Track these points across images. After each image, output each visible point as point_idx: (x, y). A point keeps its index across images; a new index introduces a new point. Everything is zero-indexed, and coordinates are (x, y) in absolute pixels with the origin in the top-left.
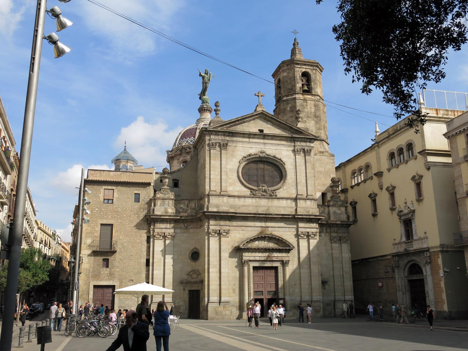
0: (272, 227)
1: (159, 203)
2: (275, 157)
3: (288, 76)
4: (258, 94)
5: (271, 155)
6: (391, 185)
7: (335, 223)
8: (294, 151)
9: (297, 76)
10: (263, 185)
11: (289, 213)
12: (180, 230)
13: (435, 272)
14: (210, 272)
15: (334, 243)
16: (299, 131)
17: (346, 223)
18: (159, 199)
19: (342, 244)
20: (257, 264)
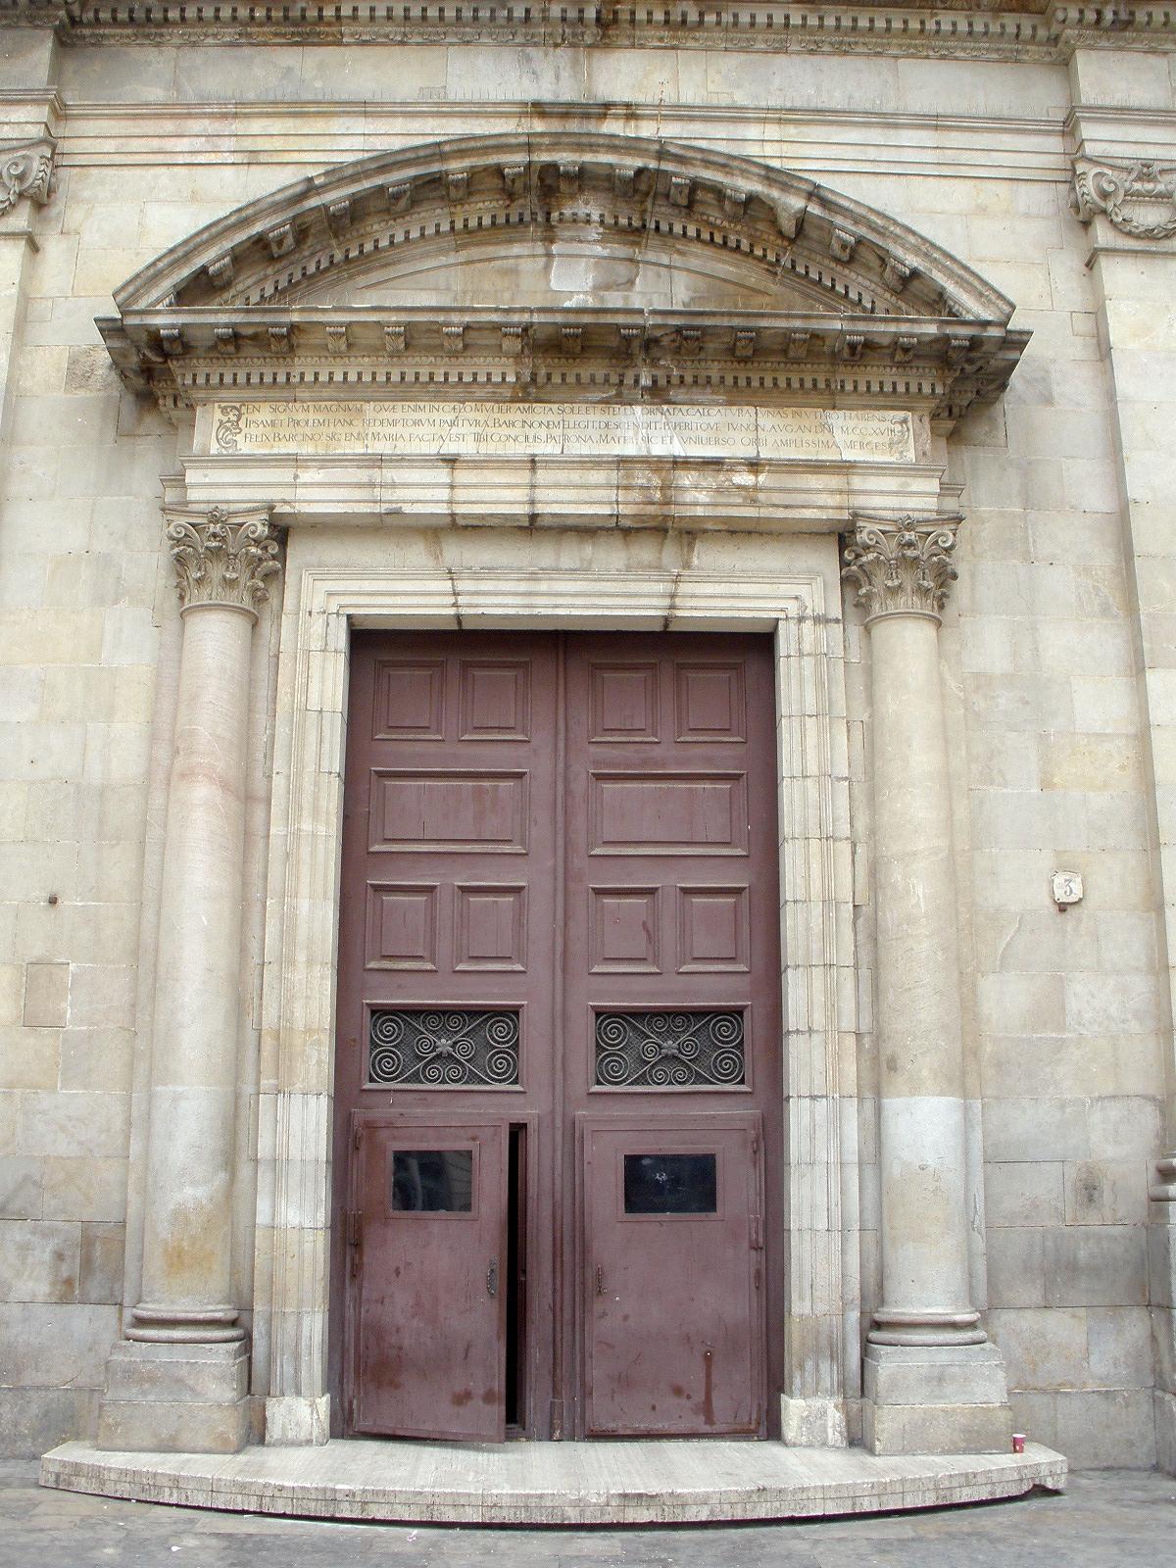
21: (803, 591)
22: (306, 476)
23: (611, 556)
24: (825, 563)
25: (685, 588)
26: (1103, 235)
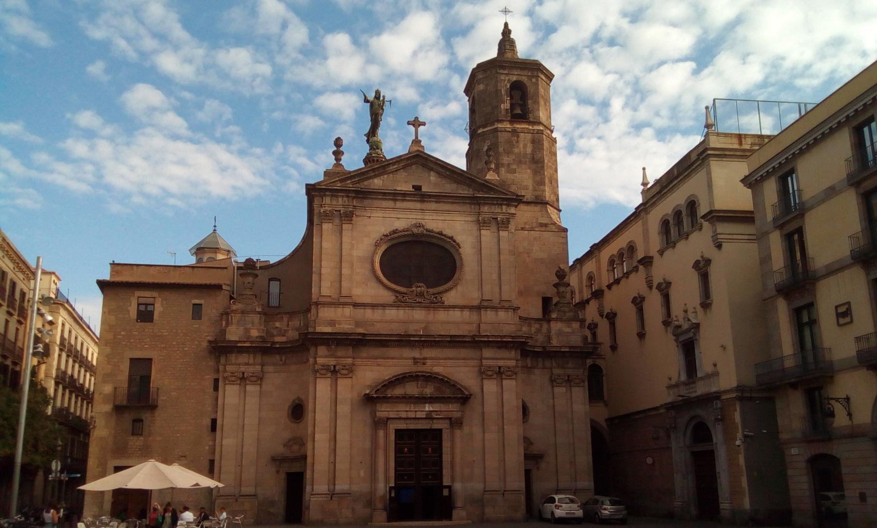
0: (432, 358)
1: (236, 318)
2: (441, 233)
3: (487, 89)
4: (413, 123)
5: (435, 230)
6: (664, 279)
7: (559, 350)
8: (478, 222)
9: (501, 90)
10: (421, 284)
11: (466, 333)
12: (272, 367)
13: (729, 438)
14: (316, 440)
15: (557, 386)
16: (487, 187)
17: (579, 350)
18: (235, 313)
19: (573, 389)
20: (402, 426)
21: (445, 425)
22: (391, 413)
23: (424, 421)
24: (448, 421)
25: (433, 425)
26: (484, 376)
